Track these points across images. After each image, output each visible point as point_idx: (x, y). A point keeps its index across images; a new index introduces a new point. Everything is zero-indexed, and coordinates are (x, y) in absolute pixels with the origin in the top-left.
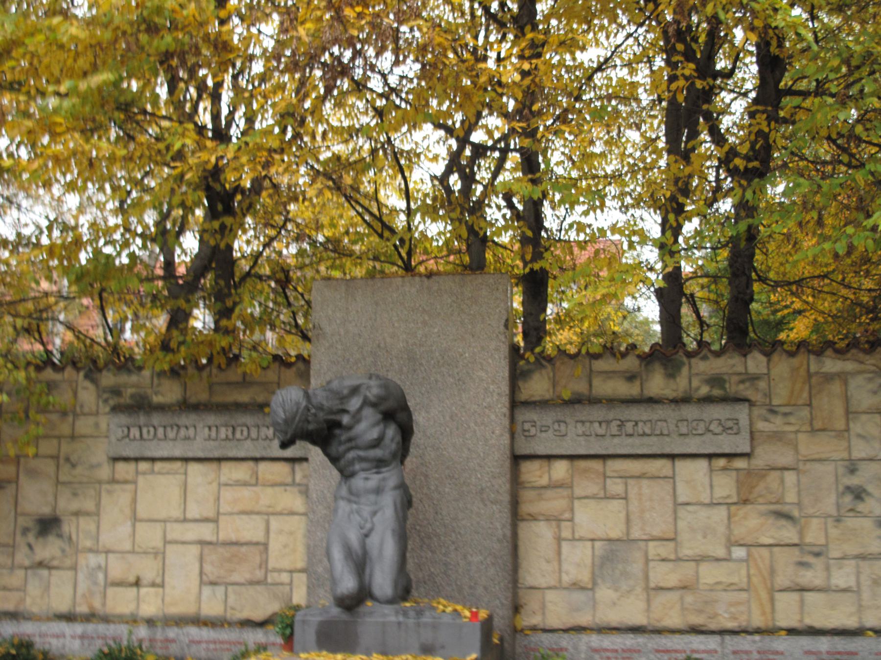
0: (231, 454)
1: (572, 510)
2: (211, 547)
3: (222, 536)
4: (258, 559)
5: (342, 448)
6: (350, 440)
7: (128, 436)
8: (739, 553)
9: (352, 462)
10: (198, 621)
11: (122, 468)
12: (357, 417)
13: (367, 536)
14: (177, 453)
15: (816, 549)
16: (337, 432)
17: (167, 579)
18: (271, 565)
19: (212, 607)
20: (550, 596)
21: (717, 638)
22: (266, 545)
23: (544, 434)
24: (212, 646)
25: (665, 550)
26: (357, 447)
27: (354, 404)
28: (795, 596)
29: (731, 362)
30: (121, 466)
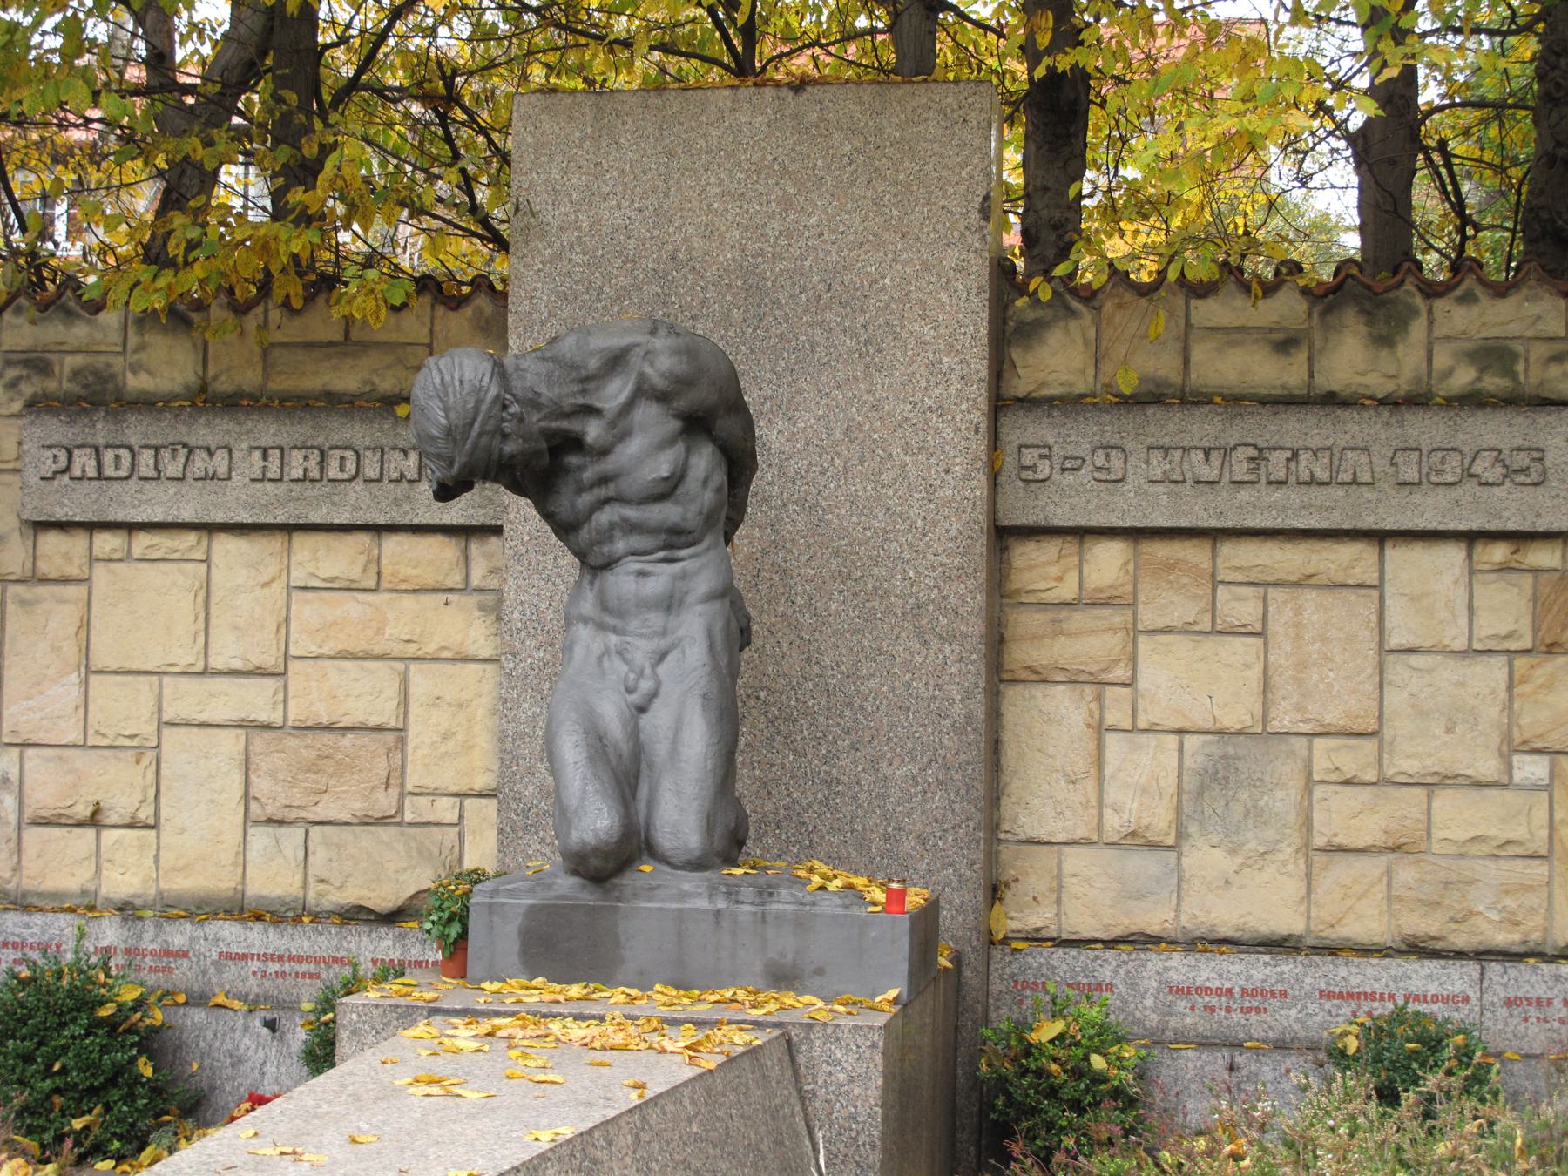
0: (315, 517)
1: (1133, 660)
2: (269, 734)
3: (295, 713)
5: (585, 500)
6: (604, 480)
7: (67, 470)
8: (1532, 769)
9: (607, 535)
12: (620, 426)
13: (642, 709)
14: (187, 514)
16: (573, 460)
17: (164, 814)
19: (273, 873)
20: (1074, 860)
21: (1472, 968)
22: (400, 731)
23: (1069, 478)
24: (273, 967)
25: (1355, 758)
26: (620, 499)
27: (615, 393)
29: (1532, 309)
30: (52, 542)
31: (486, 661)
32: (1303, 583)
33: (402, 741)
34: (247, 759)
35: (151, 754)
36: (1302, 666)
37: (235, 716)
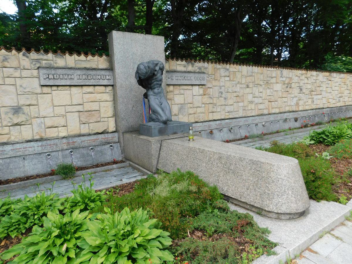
0: (87, 84)
6: (155, 79)
7: (48, 77)
8: (203, 105)
9: (155, 85)
10: (80, 135)
11: (46, 90)
13: (161, 105)
18: (102, 116)
19: (85, 130)
24: (89, 141)
25: (191, 105)
28: (212, 113)
31: (109, 101)
32: (187, 89)
33: (100, 112)
35: (65, 117)
36: (187, 97)
37: (77, 111)
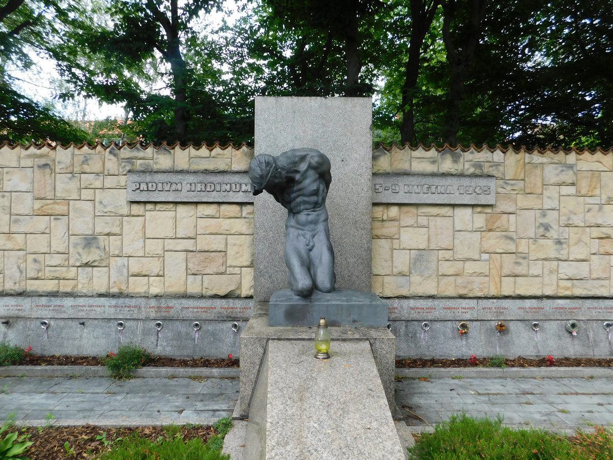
1: (399, 233)
4: (221, 261)
6: (299, 190)
9: (299, 204)
10: (185, 296)
11: (136, 209)
12: (304, 175)
13: (310, 250)
14: (170, 200)
15: (524, 255)
17: (165, 273)
18: (229, 264)
19: (194, 287)
20: (387, 279)
21: (475, 301)
23: (386, 192)
24: (195, 310)
25: (448, 254)
26: (304, 195)
27: (303, 167)
28: (512, 279)
29: (486, 155)
30: (134, 207)
31: (247, 235)
32: (437, 215)
33: (226, 254)
34: (187, 259)
35: (162, 259)
36: (437, 235)
37: (184, 249)
